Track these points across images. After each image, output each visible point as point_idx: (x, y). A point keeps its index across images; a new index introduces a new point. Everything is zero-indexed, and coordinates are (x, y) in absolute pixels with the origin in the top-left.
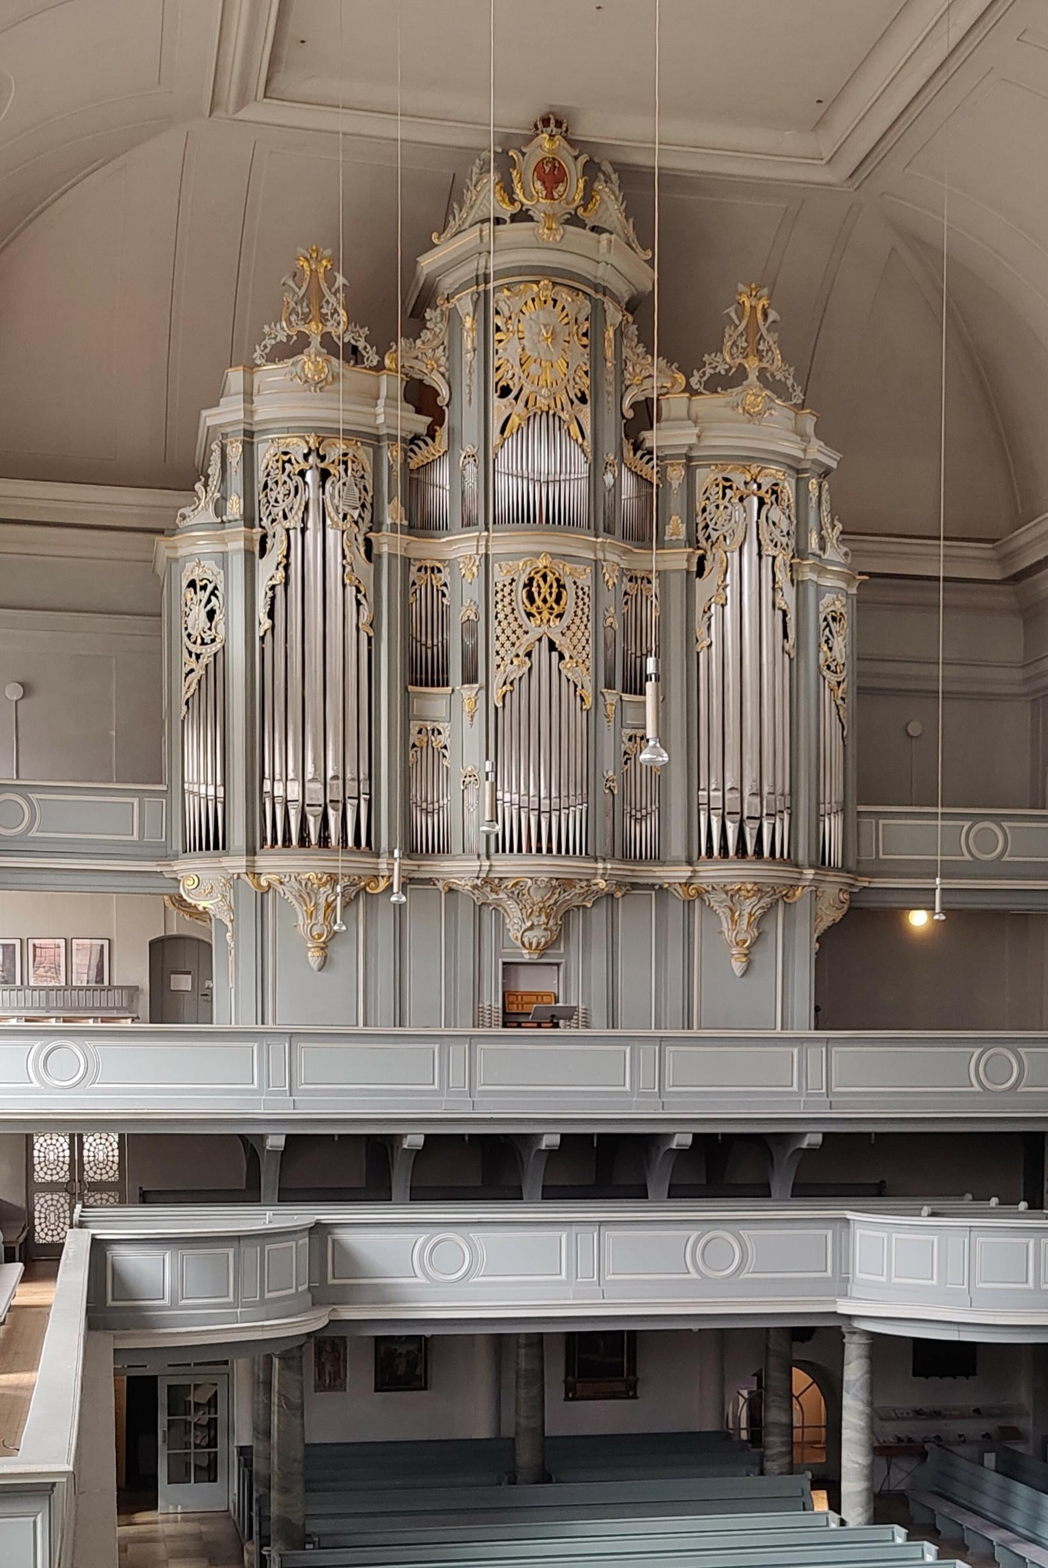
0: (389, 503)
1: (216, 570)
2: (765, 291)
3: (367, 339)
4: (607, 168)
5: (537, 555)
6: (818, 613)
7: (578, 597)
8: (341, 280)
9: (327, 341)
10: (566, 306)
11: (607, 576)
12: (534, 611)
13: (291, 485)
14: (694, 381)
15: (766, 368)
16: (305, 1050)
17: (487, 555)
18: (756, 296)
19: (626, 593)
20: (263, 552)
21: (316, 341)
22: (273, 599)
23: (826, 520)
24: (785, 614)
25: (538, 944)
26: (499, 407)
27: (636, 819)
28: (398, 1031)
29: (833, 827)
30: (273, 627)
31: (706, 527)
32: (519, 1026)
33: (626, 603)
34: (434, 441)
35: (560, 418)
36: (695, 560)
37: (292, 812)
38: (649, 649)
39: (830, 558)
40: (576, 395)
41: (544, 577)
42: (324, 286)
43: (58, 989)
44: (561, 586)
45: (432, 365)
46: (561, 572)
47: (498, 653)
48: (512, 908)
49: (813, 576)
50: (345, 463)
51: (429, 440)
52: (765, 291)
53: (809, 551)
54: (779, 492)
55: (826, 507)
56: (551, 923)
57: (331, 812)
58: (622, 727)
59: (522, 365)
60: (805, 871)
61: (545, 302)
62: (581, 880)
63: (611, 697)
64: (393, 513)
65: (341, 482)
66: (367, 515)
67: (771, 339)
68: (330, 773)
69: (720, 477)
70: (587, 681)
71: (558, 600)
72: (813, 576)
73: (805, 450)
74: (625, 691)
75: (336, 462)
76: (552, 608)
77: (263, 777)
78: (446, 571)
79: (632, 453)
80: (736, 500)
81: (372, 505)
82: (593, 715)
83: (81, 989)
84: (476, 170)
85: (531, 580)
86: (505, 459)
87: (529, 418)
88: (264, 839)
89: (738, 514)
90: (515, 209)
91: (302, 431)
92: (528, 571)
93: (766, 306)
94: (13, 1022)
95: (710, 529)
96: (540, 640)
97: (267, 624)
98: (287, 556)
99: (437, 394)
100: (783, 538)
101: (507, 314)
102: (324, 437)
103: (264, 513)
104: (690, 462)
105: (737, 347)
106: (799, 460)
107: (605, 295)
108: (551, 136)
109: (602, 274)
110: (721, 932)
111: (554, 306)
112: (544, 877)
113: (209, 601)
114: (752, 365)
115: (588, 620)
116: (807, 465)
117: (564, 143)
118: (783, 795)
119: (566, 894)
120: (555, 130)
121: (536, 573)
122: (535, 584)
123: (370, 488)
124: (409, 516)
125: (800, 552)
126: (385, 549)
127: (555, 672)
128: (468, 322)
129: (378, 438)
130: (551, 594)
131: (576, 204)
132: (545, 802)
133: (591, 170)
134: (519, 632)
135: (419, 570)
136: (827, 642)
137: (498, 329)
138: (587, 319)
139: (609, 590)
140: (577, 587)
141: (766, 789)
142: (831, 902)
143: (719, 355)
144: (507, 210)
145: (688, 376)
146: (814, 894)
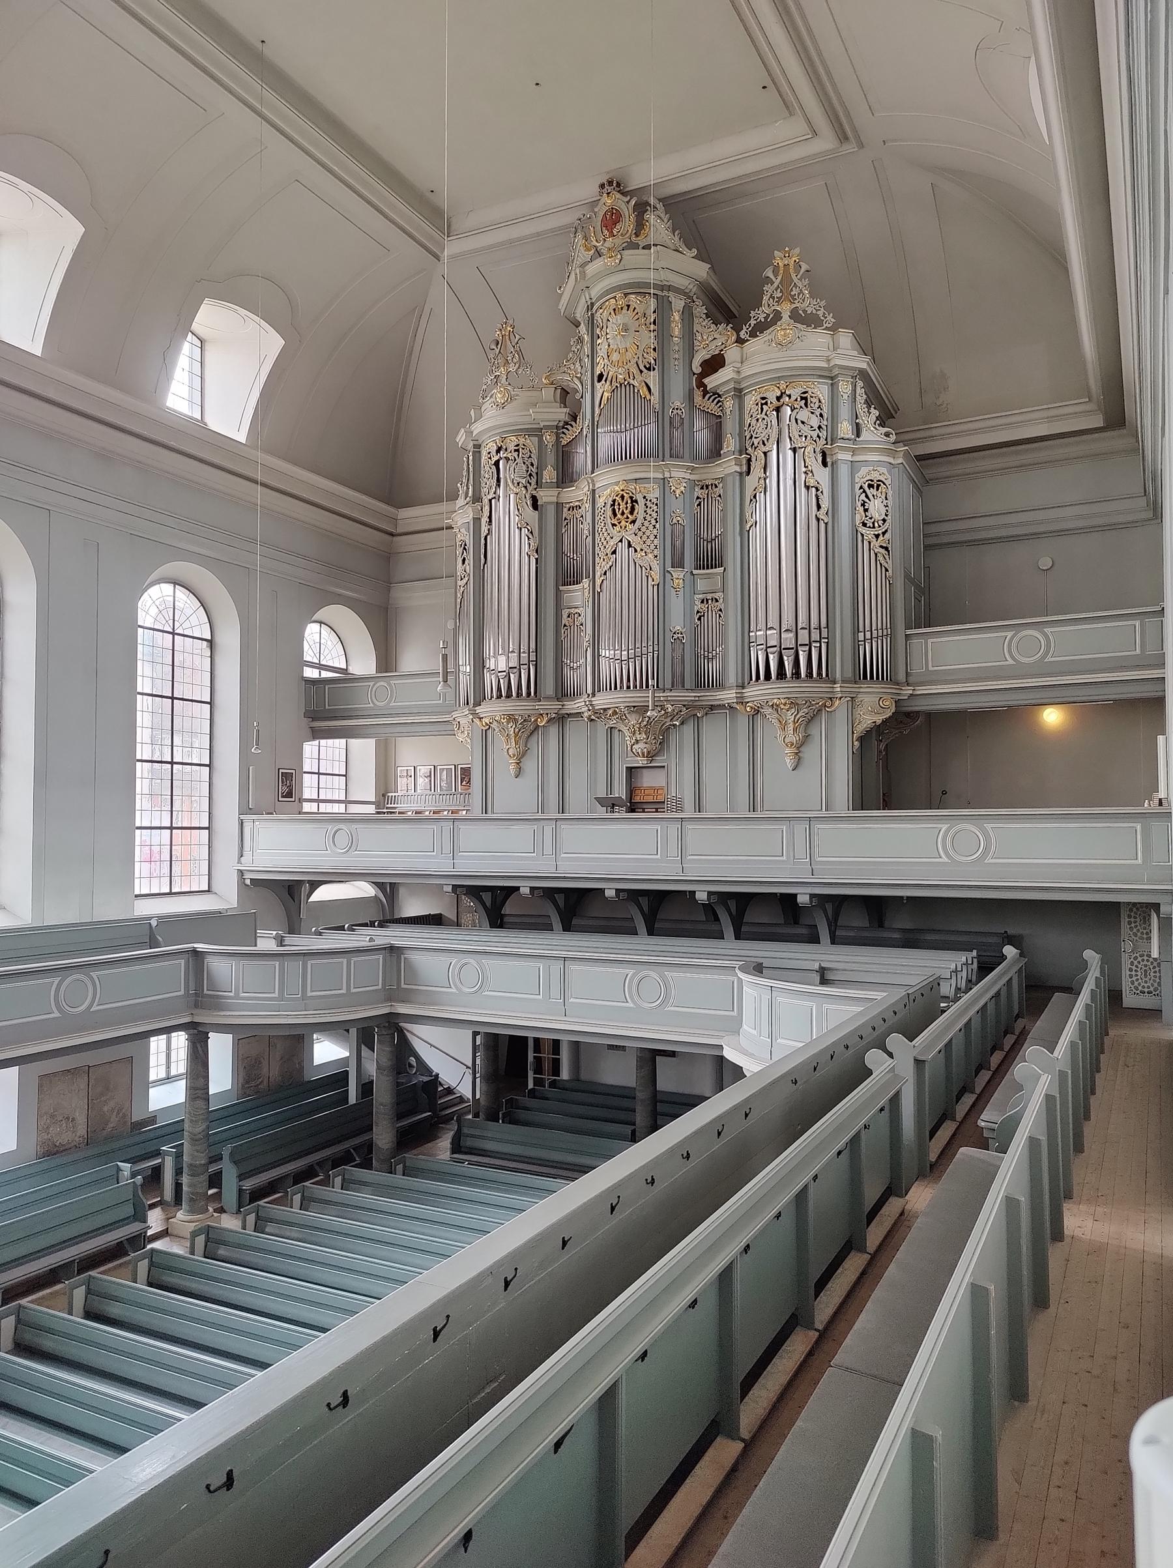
4: (652, 201)
7: (647, 507)
10: (637, 307)
11: (673, 488)
12: (616, 523)
14: (742, 334)
18: (789, 256)
19: (698, 498)
24: (817, 490)
27: (708, 659)
31: (751, 437)
33: (699, 505)
35: (634, 386)
36: (744, 462)
38: (717, 535)
40: (645, 367)
41: (623, 497)
44: (634, 501)
45: (572, 374)
46: (634, 492)
47: (598, 554)
49: (847, 456)
50: (518, 451)
51: (573, 423)
52: (797, 251)
54: (809, 397)
59: (608, 356)
61: (622, 308)
63: (677, 574)
64: (549, 474)
65: (516, 462)
66: (533, 481)
71: (632, 513)
73: (828, 361)
75: (513, 451)
76: (628, 518)
78: (583, 508)
81: (537, 473)
82: (661, 588)
92: (613, 494)
96: (621, 541)
102: (505, 437)
105: (774, 298)
106: (830, 369)
111: (628, 310)
112: (622, 706)
114: (785, 309)
115: (657, 522)
116: (836, 371)
117: (618, 195)
121: (617, 496)
122: (616, 504)
130: (627, 508)
132: (625, 653)
135: (569, 510)
136: (863, 505)
138: (654, 312)
139: (677, 498)
140: (647, 500)
142: (870, 708)
145: (737, 330)
146: (850, 703)
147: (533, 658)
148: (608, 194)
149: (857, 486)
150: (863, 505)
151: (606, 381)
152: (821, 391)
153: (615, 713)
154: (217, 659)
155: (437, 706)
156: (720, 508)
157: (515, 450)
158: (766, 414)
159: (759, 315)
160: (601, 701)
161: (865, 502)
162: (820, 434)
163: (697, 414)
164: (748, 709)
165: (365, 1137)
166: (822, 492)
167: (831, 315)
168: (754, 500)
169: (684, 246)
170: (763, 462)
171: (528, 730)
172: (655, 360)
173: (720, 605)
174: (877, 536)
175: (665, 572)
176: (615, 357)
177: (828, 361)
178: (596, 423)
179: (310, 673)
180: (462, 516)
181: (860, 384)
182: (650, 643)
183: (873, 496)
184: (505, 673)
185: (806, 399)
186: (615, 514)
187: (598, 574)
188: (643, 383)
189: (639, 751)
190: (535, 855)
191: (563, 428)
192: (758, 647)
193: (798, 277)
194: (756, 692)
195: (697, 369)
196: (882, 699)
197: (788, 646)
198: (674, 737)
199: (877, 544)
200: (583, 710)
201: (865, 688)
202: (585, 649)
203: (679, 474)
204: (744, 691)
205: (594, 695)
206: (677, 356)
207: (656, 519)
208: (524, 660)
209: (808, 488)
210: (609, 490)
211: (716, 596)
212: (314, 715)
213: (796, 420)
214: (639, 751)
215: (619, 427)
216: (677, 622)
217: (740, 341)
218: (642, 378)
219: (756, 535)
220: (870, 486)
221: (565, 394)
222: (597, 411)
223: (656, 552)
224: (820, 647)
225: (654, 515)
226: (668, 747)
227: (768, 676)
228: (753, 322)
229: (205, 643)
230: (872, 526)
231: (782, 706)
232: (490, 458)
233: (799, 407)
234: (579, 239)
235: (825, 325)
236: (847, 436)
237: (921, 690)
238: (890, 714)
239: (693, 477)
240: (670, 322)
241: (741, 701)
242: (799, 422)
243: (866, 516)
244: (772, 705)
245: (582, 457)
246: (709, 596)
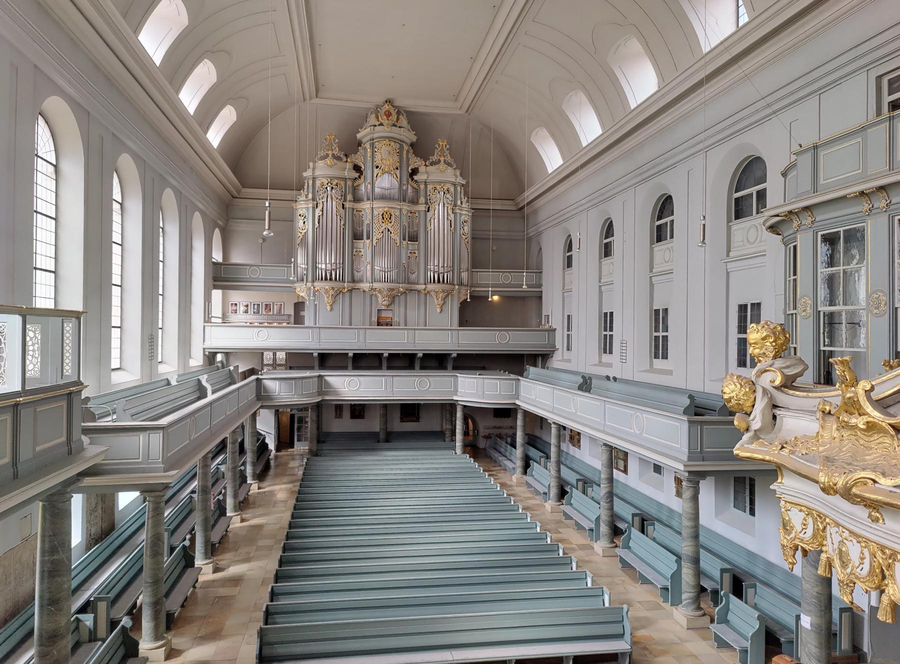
0: (349, 194)
1: (306, 212)
2: (446, 141)
3: (343, 155)
4: (403, 113)
5: (385, 207)
6: (460, 220)
8: (337, 141)
9: (333, 155)
13: (324, 191)
16: (322, 331)
17: (372, 208)
20: (317, 207)
21: (330, 155)
22: (319, 219)
23: (463, 197)
24: (451, 221)
26: (376, 171)
28: (350, 327)
29: (465, 275)
30: (319, 226)
31: (430, 199)
32: (382, 325)
36: (427, 208)
37: (323, 272)
41: (387, 213)
42: (333, 142)
43: (271, 315)
44: (391, 215)
55: (462, 194)
63: (404, 243)
64: (349, 197)
66: (343, 198)
67: (447, 152)
68: (333, 262)
69: (433, 186)
70: (398, 239)
71: (390, 219)
72: (459, 211)
73: (456, 180)
74: (409, 241)
77: (316, 263)
80: (437, 193)
83: (275, 315)
84: (370, 113)
85: (383, 214)
86: (377, 184)
88: (316, 278)
89: (438, 196)
91: (326, 178)
94: (256, 324)
96: (385, 229)
97: (318, 225)
98: (323, 208)
99: (361, 167)
103: (317, 198)
104: (426, 183)
106: (455, 182)
108: (388, 105)
109: (402, 138)
112: (386, 288)
114: (442, 159)
118: (450, 267)
123: (344, 191)
124: (354, 198)
125: (455, 205)
126: (347, 206)
127: (389, 237)
128: (369, 150)
129: (346, 179)
132: (386, 269)
133: (399, 113)
134: (380, 227)
136: (463, 228)
137: (376, 152)
141: (445, 265)
144: (377, 123)
145: (426, 162)
151: (380, 169)
152: (452, 189)
157: (336, 185)
160: (376, 285)
163: (409, 186)
171: (338, 293)
174: (466, 238)
176: (384, 161)
186: (383, 218)
187: (375, 239)
189: (385, 304)
198: (397, 300)
199: (466, 241)
203: (406, 207)
210: (381, 210)
212: (215, 279)
219: (431, 235)
220: (465, 222)
221: (357, 168)
222: (375, 178)
237: (477, 289)
239: (408, 209)
246: (413, 251)
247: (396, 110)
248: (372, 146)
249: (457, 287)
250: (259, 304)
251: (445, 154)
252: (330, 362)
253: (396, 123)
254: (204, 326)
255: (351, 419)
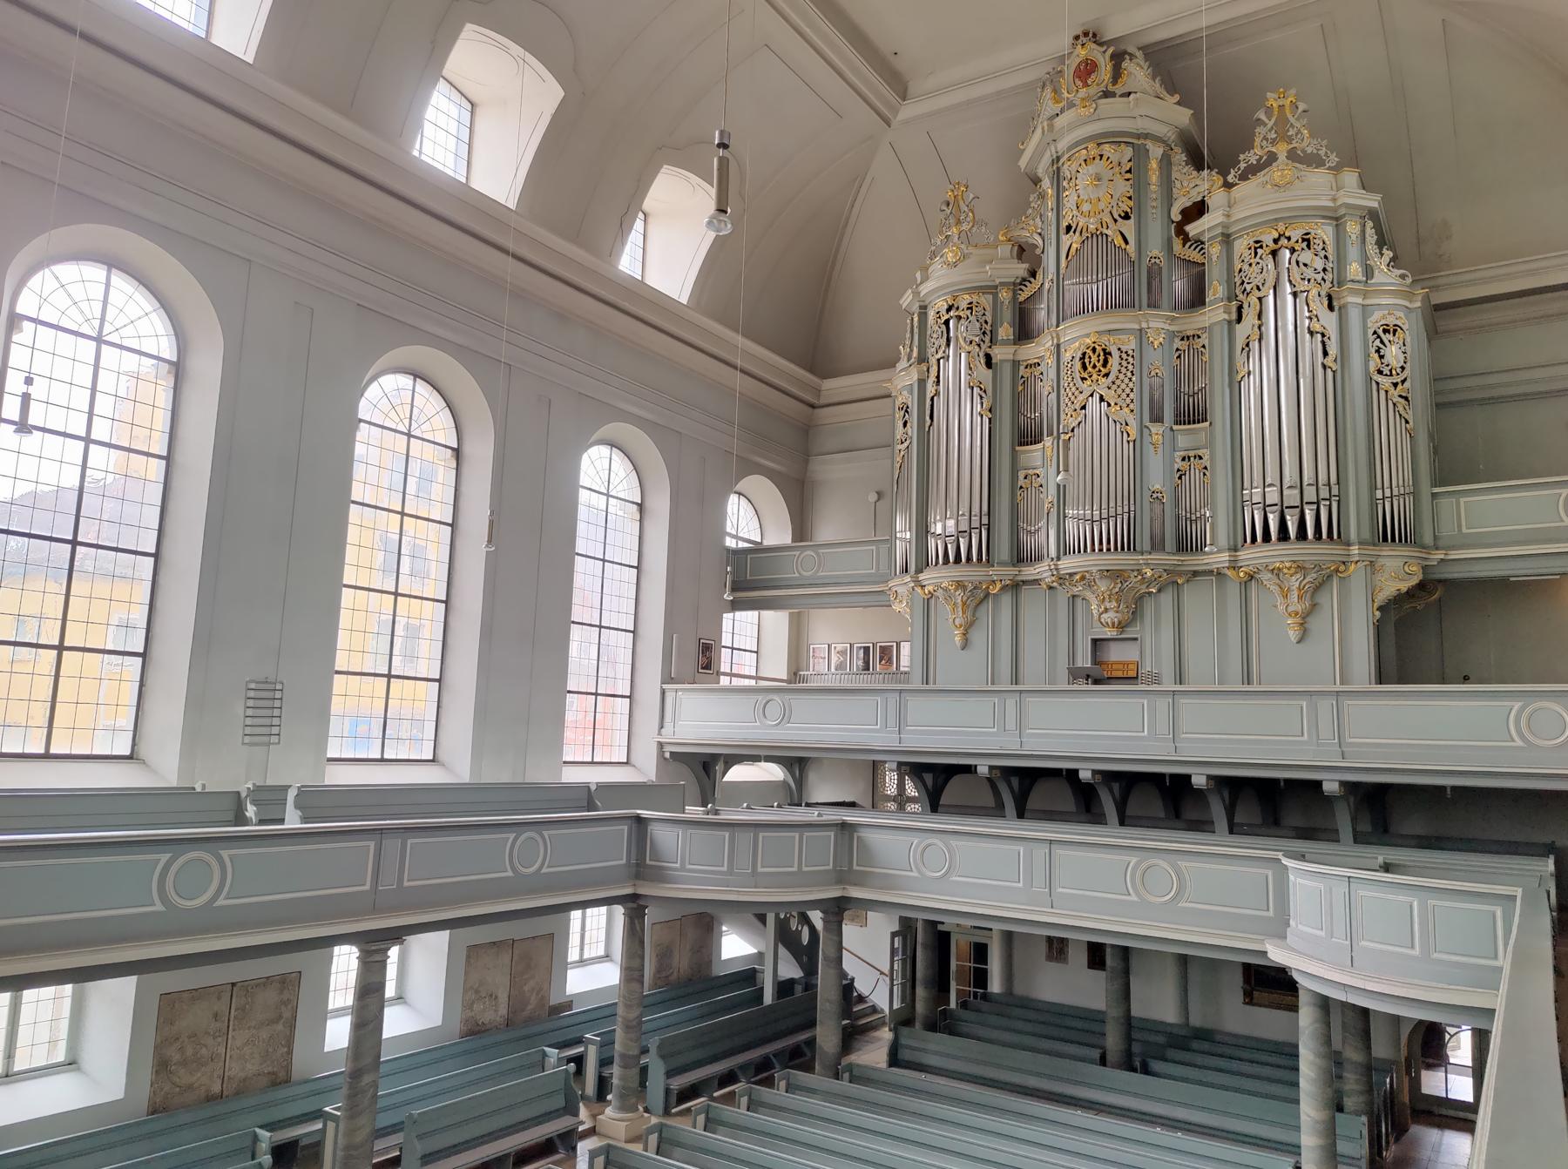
2: (1293, 91)
4: (1131, 49)
5: (1088, 335)
6: (1365, 328)
7: (1122, 359)
12: (1086, 376)
13: (940, 331)
14: (1230, 178)
15: (1296, 147)
19: (1177, 350)
24: (1323, 335)
25: (1113, 623)
26: (1066, 240)
27: (1191, 521)
31: (1243, 283)
33: (1179, 357)
34: (1035, 279)
35: (1107, 235)
36: (1234, 310)
39: (1378, 282)
40: (1120, 216)
41: (1094, 350)
44: (1107, 354)
47: (1064, 410)
48: (1088, 594)
51: (1032, 280)
52: (1293, 91)
53: (1348, 279)
56: (1121, 607)
57: (960, 539)
58: (1174, 450)
59: (1078, 208)
60: (1351, 548)
61: (1094, 158)
62: (1133, 571)
63: (1156, 429)
64: (1005, 331)
66: (987, 339)
71: (1105, 365)
72: (1359, 300)
73: (1334, 200)
76: (1100, 371)
79: (1181, 246)
81: (991, 331)
87: (1083, 242)
90: (1064, 103)
93: (1294, 101)
95: (1245, 284)
96: (1092, 395)
99: (1037, 247)
100: (1317, 276)
101: (1069, 177)
105: (1267, 140)
106: (1335, 209)
107: (1145, 139)
110: (1276, 606)
111: (1101, 160)
112: (1094, 569)
113: (905, 415)
114: (1281, 150)
115: (1133, 375)
116: (1342, 211)
117: (1094, 46)
119: (1128, 583)
120: (1085, 40)
121: (1088, 348)
122: (1087, 356)
130: (1099, 361)
131: (1105, 82)
134: (1077, 393)
135: (1026, 367)
138: (1130, 160)
140: (1122, 352)
142: (1393, 574)
143: (1252, 151)
147: (985, 521)
148: (1083, 45)
149: (1371, 332)
150: (1378, 351)
151: (1074, 232)
152: (1325, 233)
153: (1083, 578)
154: (646, 523)
155: (870, 575)
156: (1204, 359)
157: (968, 308)
158: (1261, 258)
159: (1251, 157)
160: (1068, 564)
161: (1379, 348)
162: (1326, 277)
164: (1242, 574)
165: (802, 1037)
166: (1329, 338)
167: (1335, 154)
168: (1247, 349)
169: (1165, 93)
170: (1258, 308)
171: (978, 598)
172: (1131, 209)
173: (1206, 461)
174: (1395, 385)
175: (1142, 427)
176: (1086, 207)
177: (1334, 200)
178: (1061, 276)
179: (730, 543)
180: (904, 379)
181: (1370, 224)
182: (1126, 502)
183: (1390, 341)
184: (953, 538)
185: (1308, 240)
186: (1084, 367)
188: (1118, 233)
189: (1109, 620)
190: (995, 730)
191: (1021, 284)
192: (1254, 506)
193: (1296, 117)
194: (1252, 556)
195: (1177, 217)
196: (1407, 564)
197: (1292, 505)
199: (1396, 393)
200: (1045, 575)
201: (1386, 550)
202: (1046, 511)
203: (1158, 324)
204: (1238, 554)
205: (1059, 559)
206: (1154, 204)
207: (1132, 372)
208: (976, 524)
209: (1311, 333)
210: (1077, 344)
211: (1200, 452)
213: (1297, 262)
214: (1109, 620)
215: (1089, 277)
216: (1157, 480)
217: (1228, 186)
218: (1115, 227)
220: (1385, 331)
221: (1022, 251)
223: (1132, 406)
224: (1330, 506)
225: (1130, 367)
226: (1142, 617)
227: (1267, 537)
228: (1243, 165)
229: (635, 506)
230: (1389, 374)
231: (1285, 571)
232: (940, 317)
233: (1300, 249)
234: (1048, 91)
235: (1328, 165)
236: (1357, 278)
237: (1454, 555)
238: (1417, 581)
240: (1147, 171)
241: (1234, 566)
242: (1301, 264)
243: (1382, 363)
244: (1273, 570)
245: (1042, 314)
246: (1192, 453)
247: (1111, 50)
248: (1057, 176)
249: (1355, 550)
250: (869, 647)
251: (1289, 134)
252: (953, 791)
253: (1110, 88)
254: (663, 692)
255: (1089, 968)
